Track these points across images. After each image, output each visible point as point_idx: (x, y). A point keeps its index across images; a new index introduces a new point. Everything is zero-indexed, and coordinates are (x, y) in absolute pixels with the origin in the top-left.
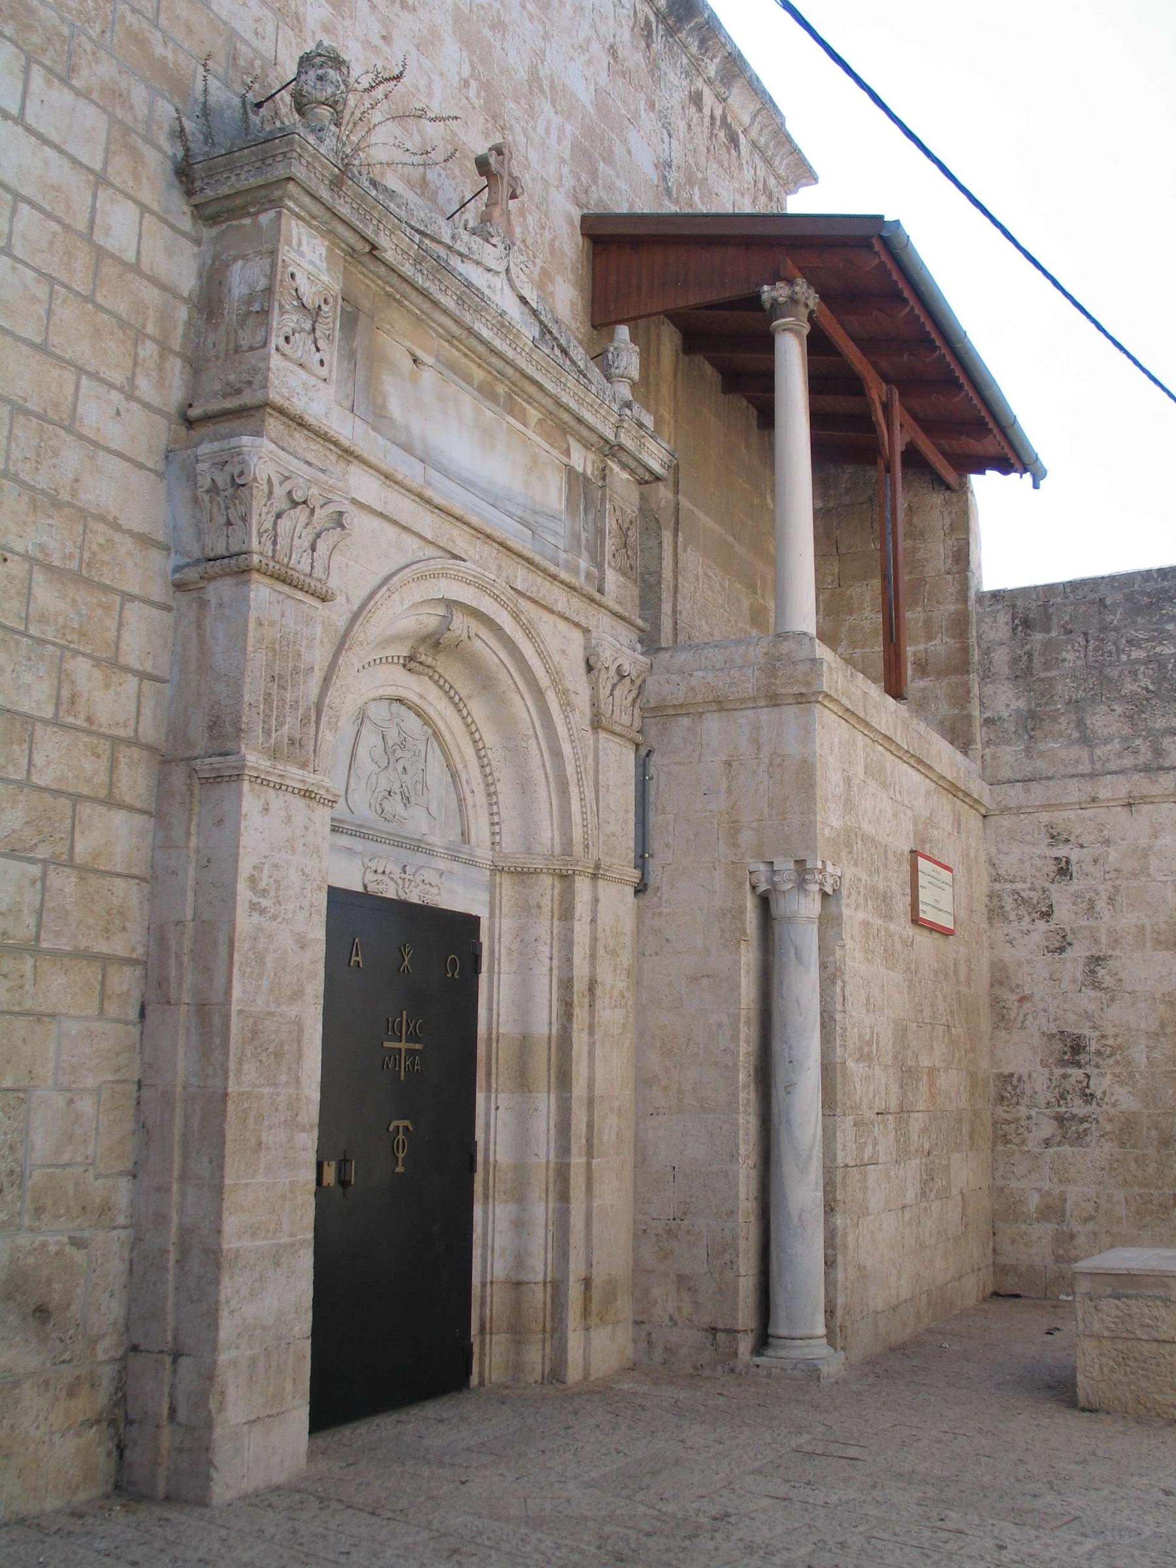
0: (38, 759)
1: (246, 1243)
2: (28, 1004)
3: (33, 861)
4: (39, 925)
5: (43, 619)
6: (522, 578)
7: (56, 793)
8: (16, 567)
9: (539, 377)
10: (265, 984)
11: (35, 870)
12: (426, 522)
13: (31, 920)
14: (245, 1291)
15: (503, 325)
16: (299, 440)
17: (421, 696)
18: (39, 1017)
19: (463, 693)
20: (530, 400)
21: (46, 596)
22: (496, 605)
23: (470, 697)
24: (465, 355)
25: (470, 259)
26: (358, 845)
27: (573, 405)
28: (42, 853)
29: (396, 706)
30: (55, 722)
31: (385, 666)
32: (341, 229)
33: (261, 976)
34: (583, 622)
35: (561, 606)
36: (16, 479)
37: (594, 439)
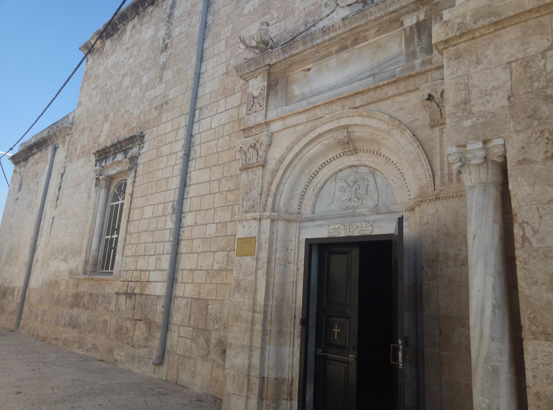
0: (228, 230)
1: (233, 341)
2: (224, 282)
3: (226, 251)
4: (227, 264)
5: (229, 201)
6: (358, 101)
7: (230, 236)
8: (224, 194)
9: (354, 26)
10: (242, 272)
11: (226, 253)
12: (302, 118)
13: (225, 263)
14: (233, 355)
15: (325, 31)
16: (254, 130)
17: (359, 161)
18: (226, 284)
19: (376, 149)
20: (366, 30)
21: (230, 196)
22: (350, 118)
23: (380, 149)
24: (327, 49)
25: (317, 22)
26: (325, 222)
27: (382, 13)
28: (228, 249)
29: (350, 170)
30: (232, 221)
31: (336, 160)
32: (259, 71)
33: (241, 270)
34: (412, 88)
35: (390, 94)
36: (225, 177)
37: (412, 7)
